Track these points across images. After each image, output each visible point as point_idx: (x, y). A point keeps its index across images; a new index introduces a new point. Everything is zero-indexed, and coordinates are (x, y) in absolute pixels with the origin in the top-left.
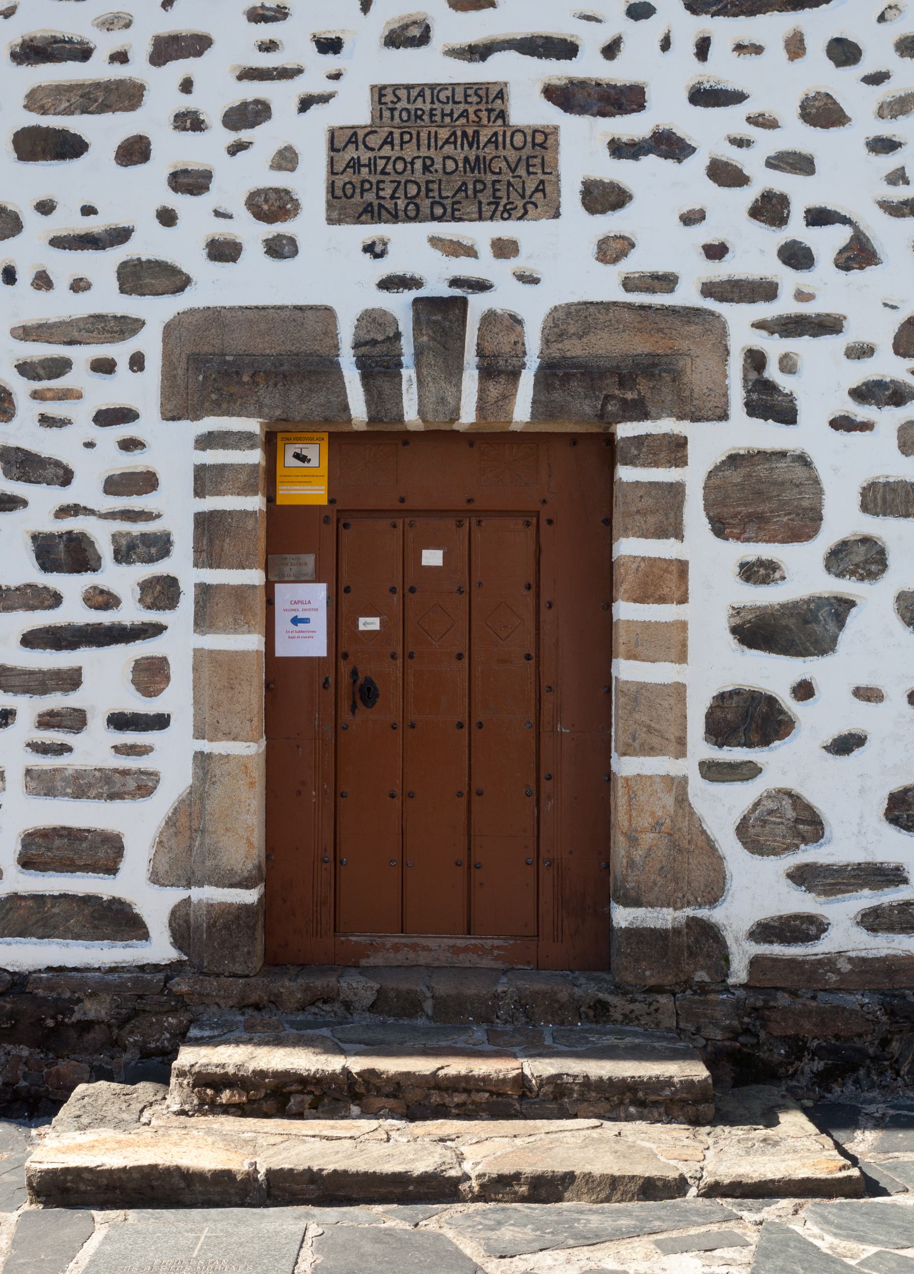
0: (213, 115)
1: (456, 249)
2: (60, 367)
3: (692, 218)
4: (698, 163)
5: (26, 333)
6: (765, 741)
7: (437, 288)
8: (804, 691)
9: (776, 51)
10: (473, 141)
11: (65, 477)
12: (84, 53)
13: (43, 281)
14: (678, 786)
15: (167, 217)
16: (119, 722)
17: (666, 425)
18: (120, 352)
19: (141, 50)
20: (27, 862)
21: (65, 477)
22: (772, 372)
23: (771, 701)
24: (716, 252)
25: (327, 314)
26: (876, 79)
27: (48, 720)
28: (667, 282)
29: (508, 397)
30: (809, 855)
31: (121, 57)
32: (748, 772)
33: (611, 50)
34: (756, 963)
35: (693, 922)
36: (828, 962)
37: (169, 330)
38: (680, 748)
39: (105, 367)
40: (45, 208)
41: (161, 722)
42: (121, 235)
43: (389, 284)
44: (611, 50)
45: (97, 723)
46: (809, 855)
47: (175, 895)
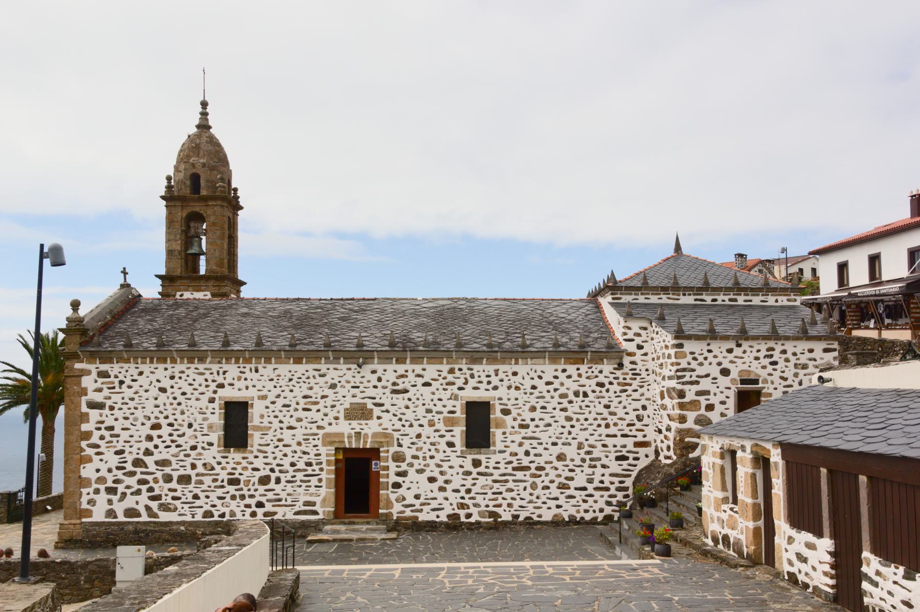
0: (329, 406)
1: (360, 424)
2: (308, 439)
3: (391, 420)
4: (391, 414)
5: (304, 435)
6: (399, 488)
7: (358, 430)
8: (404, 482)
9: (401, 399)
10: (363, 410)
11: (309, 454)
12: (312, 397)
13: (306, 428)
14: (388, 495)
15: (323, 420)
16: (316, 486)
17: (385, 448)
18: (316, 437)
19: (319, 397)
20: (304, 505)
21: (309, 454)
22: (400, 441)
23: (400, 483)
24: (393, 425)
25: (343, 434)
26: (414, 403)
27: (307, 486)
28: (387, 429)
29: (366, 445)
30: (404, 503)
31: (316, 398)
32: (396, 492)
33: (380, 398)
34: (397, 517)
35: (389, 512)
36: (406, 517)
37: (323, 435)
38: (388, 489)
39: (314, 439)
40: (306, 418)
41: (321, 487)
42: (316, 422)
43: (352, 429)
44: (380, 398)
45: (313, 487)
46: (404, 503)
47: (323, 509)
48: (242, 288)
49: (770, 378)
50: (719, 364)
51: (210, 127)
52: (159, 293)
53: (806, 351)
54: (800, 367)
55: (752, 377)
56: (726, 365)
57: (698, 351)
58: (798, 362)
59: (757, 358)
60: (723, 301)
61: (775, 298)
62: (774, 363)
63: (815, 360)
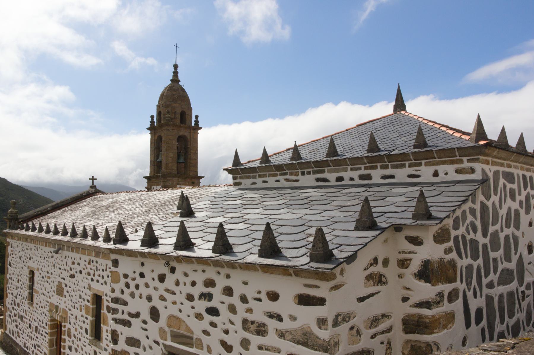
48: (201, 180)
49: (205, 340)
50: (149, 299)
51: (179, 81)
52: (146, 188)
53: (263, 296)
54: (253, 327)
55: (182, 331)
56: (157, 303)
57: (131, 275)
58: (250, 317)
59: (190, 298)
60: (352, 179)
61: (431, 169)
62: (213, 311)
63: (280, 319)
